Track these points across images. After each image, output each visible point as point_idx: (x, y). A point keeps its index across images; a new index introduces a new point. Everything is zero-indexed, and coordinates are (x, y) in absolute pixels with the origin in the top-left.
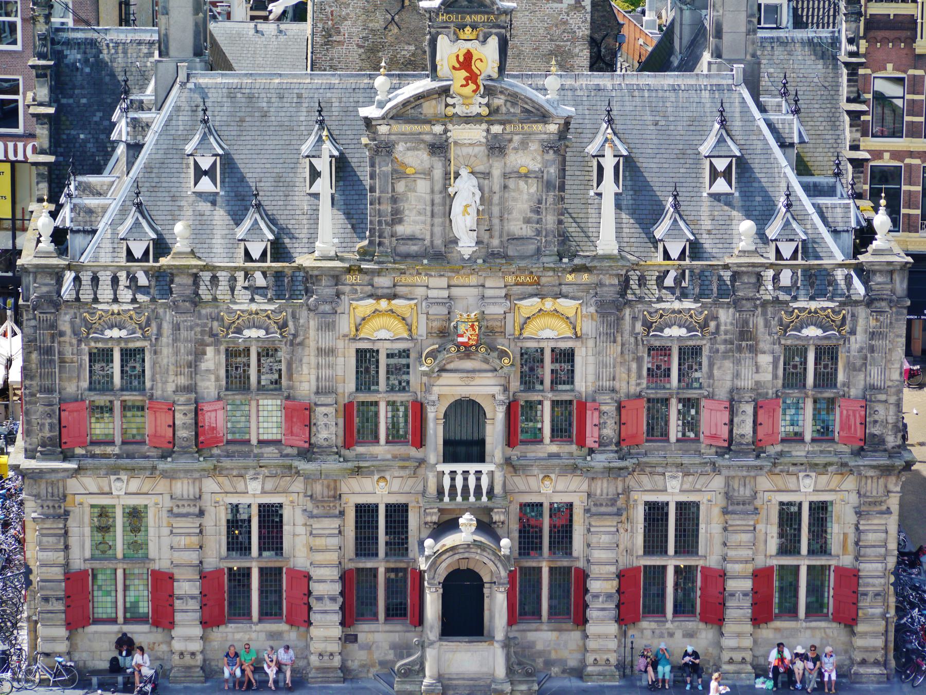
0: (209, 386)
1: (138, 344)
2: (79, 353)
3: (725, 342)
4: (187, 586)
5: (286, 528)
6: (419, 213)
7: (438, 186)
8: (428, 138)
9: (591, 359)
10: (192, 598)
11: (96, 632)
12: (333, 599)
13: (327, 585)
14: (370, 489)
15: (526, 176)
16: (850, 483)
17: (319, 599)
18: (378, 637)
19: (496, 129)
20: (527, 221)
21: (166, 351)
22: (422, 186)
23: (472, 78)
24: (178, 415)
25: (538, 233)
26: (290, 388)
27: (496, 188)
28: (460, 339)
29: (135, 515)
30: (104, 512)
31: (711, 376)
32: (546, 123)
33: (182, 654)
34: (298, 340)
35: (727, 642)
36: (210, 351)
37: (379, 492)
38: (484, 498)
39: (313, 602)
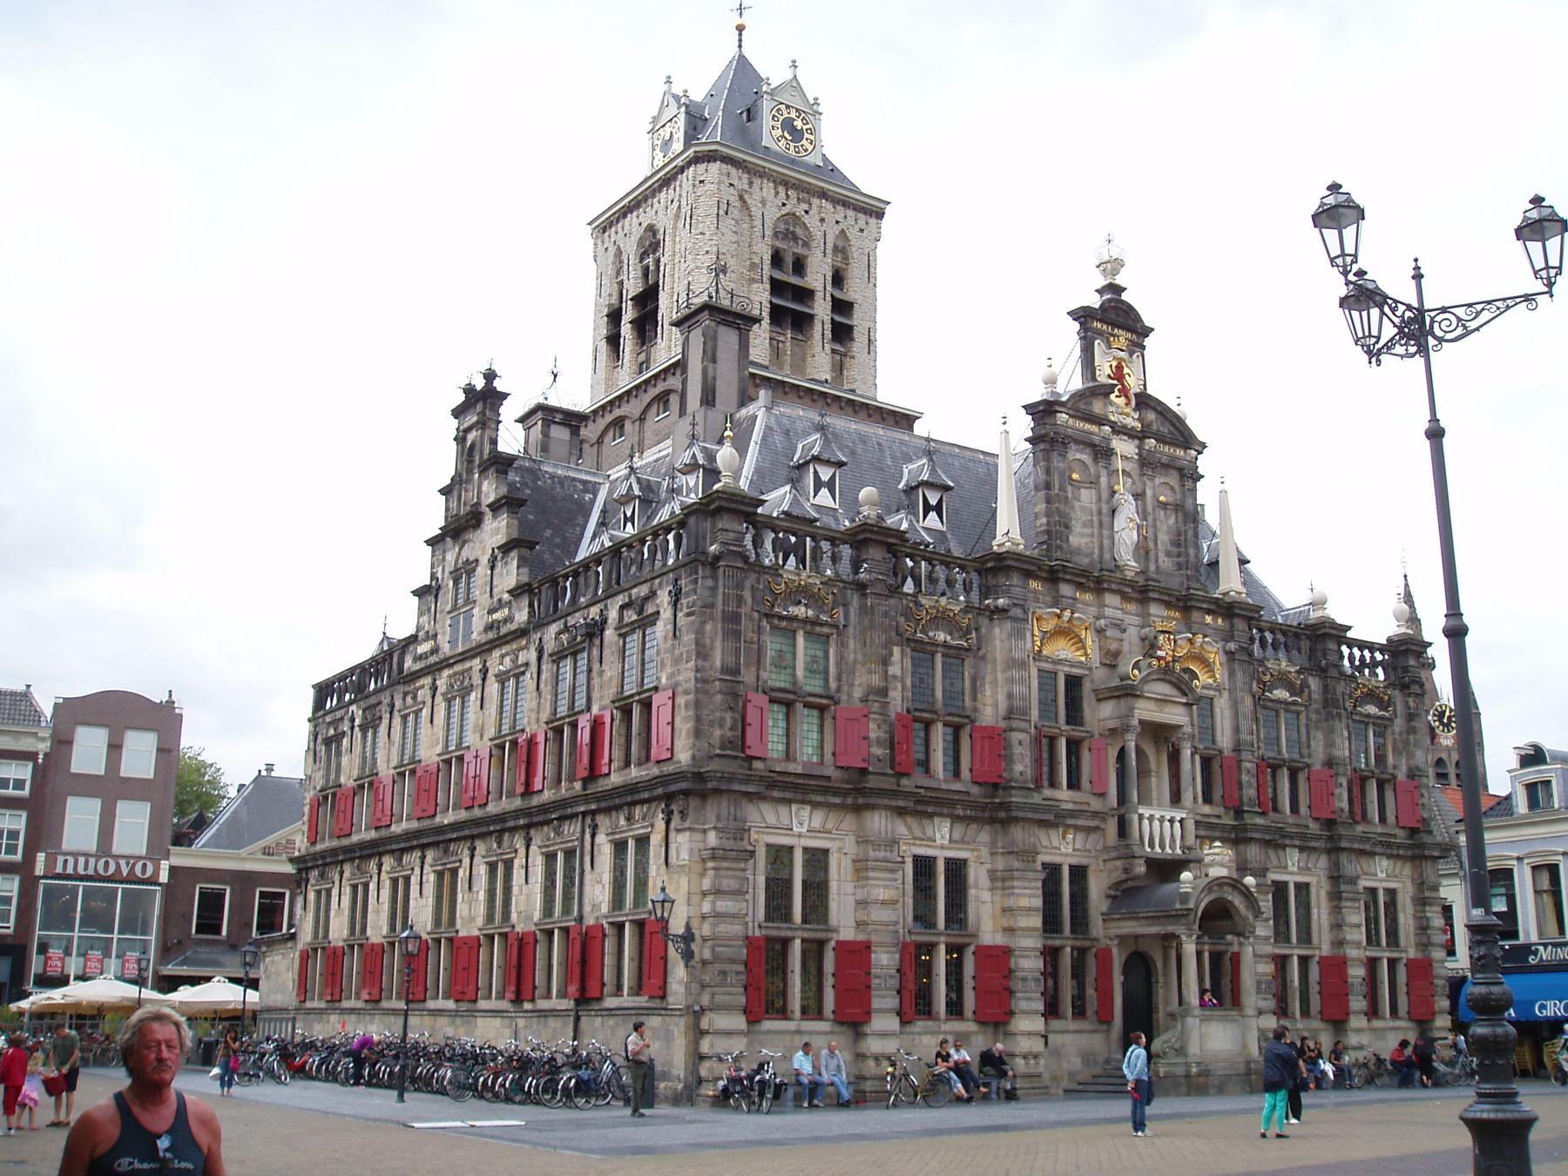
0: (897, 700)
1: (826, 630)
2: (759, 631)
3: (1318, 712)
4: (884, 960)
5: (972, 892)
6: (1085, 525)
7: (1105, 495)
8: (1096, 440)
9: (1227, 713)
10: (891, 977)
11: (769, 1032)
12: (1037, 980)
13: (1029, 964)
14: (1055, 843)
15: (1164, 506)
16: (1407, 870)
17: (1024, 979)
18: (1068, 1039)
19: (1151, 443)
20: (1168, 554)
21: (852, 644)
22: (1087, 496)
23: (1124, 392)
24: (872, 726)
25: (1179, 566)
26: (975, 710)
27: (1150, 509)
28: (1159, 653)
29: (816, 860)
30: (780, 855)
31: (1309, 746)
32: (1186, 448)
33: (877, 1059)
34: (981, 653)
35: (1353, 1039)
36: (896, 650)
37: (1063, 848)
38: (1179, 851)
39: (1012, 984)
